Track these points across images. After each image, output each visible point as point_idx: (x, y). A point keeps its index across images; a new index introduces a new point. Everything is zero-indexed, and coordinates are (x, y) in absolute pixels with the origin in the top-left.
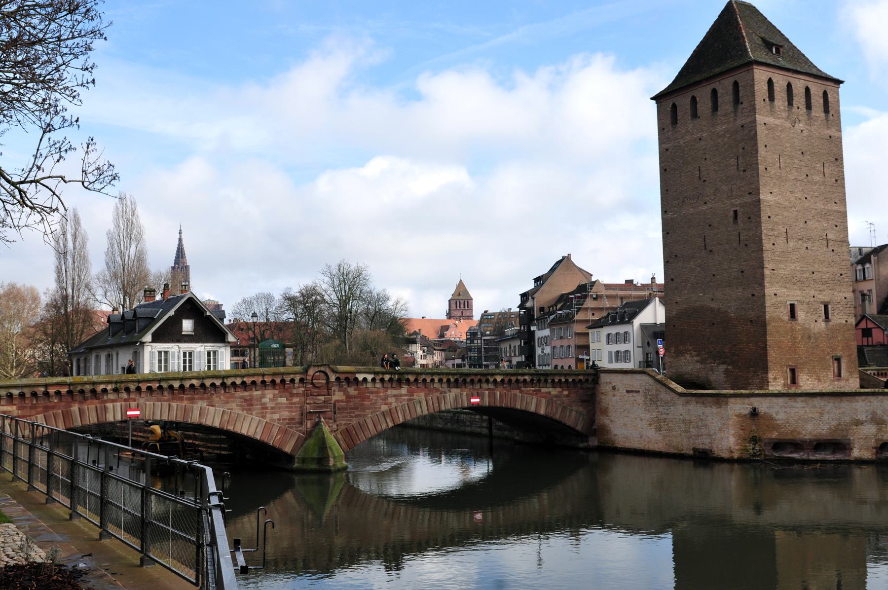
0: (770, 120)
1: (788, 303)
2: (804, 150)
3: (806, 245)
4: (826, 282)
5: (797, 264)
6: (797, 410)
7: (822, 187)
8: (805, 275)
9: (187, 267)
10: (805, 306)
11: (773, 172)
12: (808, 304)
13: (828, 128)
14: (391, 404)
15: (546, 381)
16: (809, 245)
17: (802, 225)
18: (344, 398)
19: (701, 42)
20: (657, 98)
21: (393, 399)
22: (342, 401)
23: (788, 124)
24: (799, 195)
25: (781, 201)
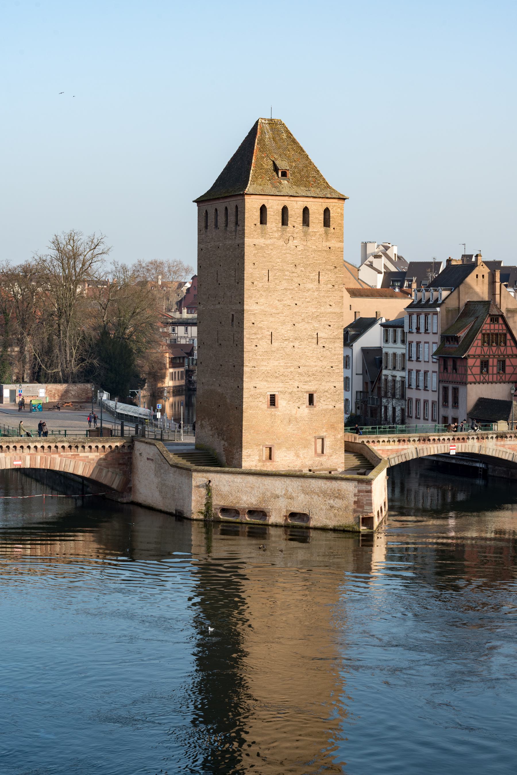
0: (261, 241)
2: (297, 262)
3: (292, 344)
4: (313, 374)
5: (281, 361)
6: (237, 485)
7: (316, 293)
11: (261, 285)
12: (290, 393)
13: (327, 240)
15: (83, 447)
16: (296, 344)
17: (289, 326)
19: (235, 155)
20: (198, 201)
23: (281, 242)
24: (288, 302)
25: (267, 309)
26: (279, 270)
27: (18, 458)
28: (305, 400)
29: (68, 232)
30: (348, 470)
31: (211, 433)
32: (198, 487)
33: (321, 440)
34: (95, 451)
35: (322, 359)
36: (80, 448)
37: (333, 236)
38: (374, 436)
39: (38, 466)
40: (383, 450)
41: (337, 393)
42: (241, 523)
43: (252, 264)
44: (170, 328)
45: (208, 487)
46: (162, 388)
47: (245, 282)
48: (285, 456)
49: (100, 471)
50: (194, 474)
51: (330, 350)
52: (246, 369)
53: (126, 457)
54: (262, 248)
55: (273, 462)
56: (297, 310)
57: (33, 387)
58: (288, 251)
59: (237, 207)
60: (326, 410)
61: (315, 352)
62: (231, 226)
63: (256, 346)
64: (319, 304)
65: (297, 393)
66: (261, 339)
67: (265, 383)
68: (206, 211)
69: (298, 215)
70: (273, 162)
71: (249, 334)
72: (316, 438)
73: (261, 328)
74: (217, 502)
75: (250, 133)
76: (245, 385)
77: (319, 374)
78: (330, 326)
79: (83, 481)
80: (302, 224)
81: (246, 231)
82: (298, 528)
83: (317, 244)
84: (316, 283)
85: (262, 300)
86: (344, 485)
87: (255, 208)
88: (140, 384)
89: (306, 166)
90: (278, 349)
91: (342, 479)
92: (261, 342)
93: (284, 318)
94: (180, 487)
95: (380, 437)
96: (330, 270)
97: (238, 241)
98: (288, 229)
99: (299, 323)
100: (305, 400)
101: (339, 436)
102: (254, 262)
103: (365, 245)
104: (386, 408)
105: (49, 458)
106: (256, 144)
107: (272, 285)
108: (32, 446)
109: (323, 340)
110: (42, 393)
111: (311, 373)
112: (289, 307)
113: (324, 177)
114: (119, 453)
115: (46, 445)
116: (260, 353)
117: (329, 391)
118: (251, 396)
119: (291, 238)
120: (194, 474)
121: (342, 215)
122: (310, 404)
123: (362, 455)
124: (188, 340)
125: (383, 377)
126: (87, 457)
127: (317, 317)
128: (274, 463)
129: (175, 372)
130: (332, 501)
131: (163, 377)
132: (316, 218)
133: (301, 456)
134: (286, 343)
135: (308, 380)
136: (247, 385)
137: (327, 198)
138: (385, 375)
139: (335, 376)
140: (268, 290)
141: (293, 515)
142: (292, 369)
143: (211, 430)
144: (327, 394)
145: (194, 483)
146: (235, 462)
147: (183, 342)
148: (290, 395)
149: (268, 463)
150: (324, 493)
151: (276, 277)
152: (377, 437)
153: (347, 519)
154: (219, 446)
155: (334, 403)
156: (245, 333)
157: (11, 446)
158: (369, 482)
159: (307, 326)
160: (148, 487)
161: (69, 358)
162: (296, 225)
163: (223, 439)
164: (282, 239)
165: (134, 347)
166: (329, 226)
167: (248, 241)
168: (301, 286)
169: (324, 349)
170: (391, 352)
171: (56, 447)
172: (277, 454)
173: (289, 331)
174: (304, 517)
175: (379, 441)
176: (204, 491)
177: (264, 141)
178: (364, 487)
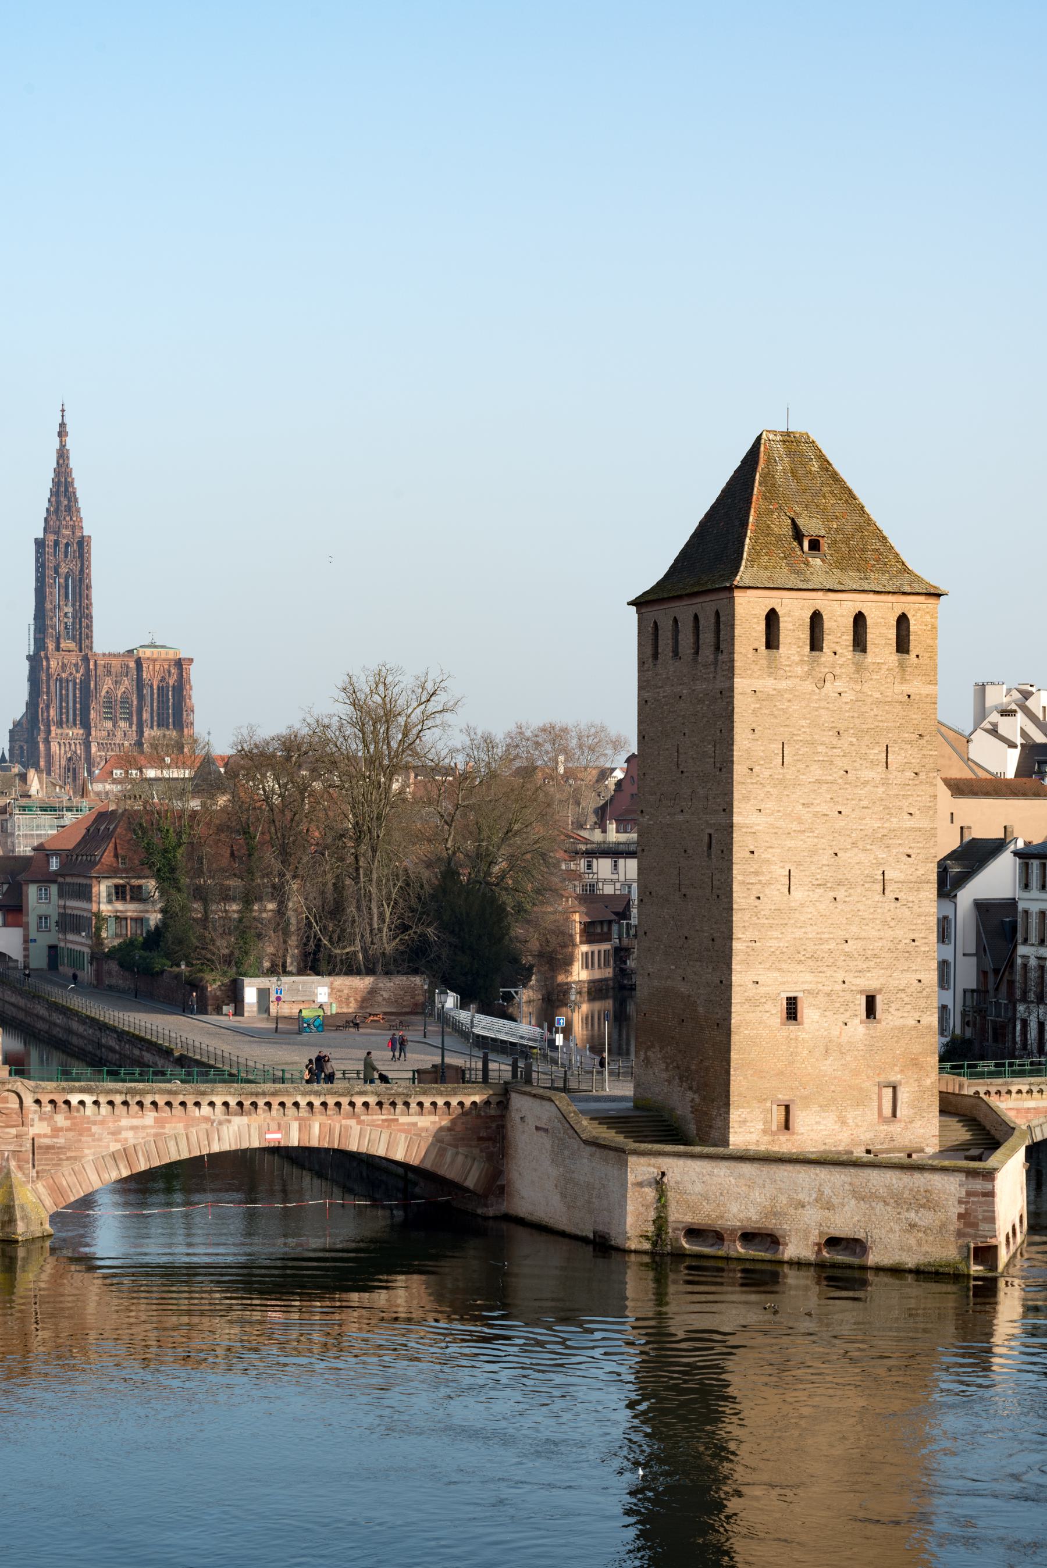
0: (767, 684)
1: (784, 995)
2: (841, 726)
3: (832, 894)
4: (875, 956)
5: (809, 929)
6: (720, 1180)
7: (881, 790)
8: (826, 947)
9: (83, 544)
10: (822, 999)
11: (767, 773)
12: (828, 995)
13: (904, 680)
14: (126, 1140)
15: (407, 1104)
16: (841, 894)
17: (826, 858)
18: (48, 1131)
19: (713, 507)
20: (639, 603)
21: (129, 1135)
22: (45, 1136)
23: (809, 686)
24: (824, 808)
26: (806, 742)
27: (274, 1126)
28: (858, 1008)
29: (374, 667)
30: (946, 1151)
31: (665, 1075)
32: (640, 1184)
33: (890, 1090)
34: (430, 1113)
35: (892, 924)
36: (400, 1107)
37: (917, 672)
38: (1000, 1081)
39: (315, 1143)
40: (1018, 1110)
41: (925, 993)
42: (727, 1259)
43: (749, 732)
44: (583, 863)
45: (659, 1184)
46: (567, 984)
47: (735, 767)
48: (818, 1123)
49: (442, 1152)
50: (632, 1160)
51: (910, 905)
52: (736, 945)
53: (494, 1125)
54: (769, 697)
55: (793, 1134)
56: (843, 824)
57: (304, 983)
58: (823, 704)
59: (717, 614)
60: (901, 1028)
61: (879, 910)
62: (707, 653)
63: (759, 898)
64: (887, 811)
65: (841, 994)
66: (769, 883)
67: (777, 974)
68: (655, 623)
69: (844, 630)
70: (793, 520)
71: (744, 873)
72: (881, 1086)
73: (767, 861)
74: (678, 1215)
75: (744, 462)
76: (736, 978)
77: (888, 955)
78: (909, 856)
79: (406, 1172)
80: (851, 648)
81: (736, 664)
82: (843, 1267)
83: (882, 689)
84: (882, 768)
85: (769, 805)
86: (937, 1180)
87: (755, 616)
88: (522, 977)
89: (860, 529)
90: (802, 905)
91: (934, 1169)
92: (767, 891)
93: (816, 840)
94: (604, 1186)
95: (1011, 1084)
96: (910, 742)
97: (720, 685)
98: (823, 659)
99: (846, 850)
100: (858, 1008)
101: (928, 1082)
102: (754, 726)
103: (981, 690)
104: (1025, 1023)
105: (338, 1126)
106: (757, 484)
107: (790, 773)
108: (303, 1103)
109: (896, 885)
110: (323, 993)
111: (869, 952)
112: (825, 818)
113: (897, 549)
114: (479, 1116)
115: (331, 1101)
116: (767, 912)
117: (908, 990)
118: (748, 1000)
119: (829, 677)
120: (632, 1160)
121: (934, 627)
122: (868, 1017)
123: (975, 1120)
124: (618, 886)
125: (1019, 961)
126: (415, 1124)
127: (882, 839)
128: (795, 1137)
129: (593, 953)
130: (912, 1215)
131: (569, 962)
132: (881, 635)
133: (850, 1121)
134: (820, 891)
135: (865, 966)
136: (741, 977)
137: (904, 593)
138: (1023, 956)
139: (919, 960)
140: (781, 782)
141: (833, 1242)
142: (832, 945)
143: (667, 1069)
144: (903, 995)
145: (631, 1178)
146: (715, 1134)
147: (608, 890)
148: (827, 999)
149: (783, 1137)
150: (898, 1200)
151: (799, 757)
152: (1006, 1084)
153: (945, 1251)
154: (681, 1103)
155: (917, 1014)
156: (734, 872)
157: (261, 1102)
158: (989, 1175)
159: (862, 856)
160: (537, 1186)
161: (376, 925)
162: (839, 651)
163: (690, 1088)
164: (810, 680)
165: (508, 901)
166: (907, 652)
167: (741, 684)
168: (849, 775)
169: (898, 904)
170: (1034, 908)
171: (352, 1104)
172: (801, 1119)
173: (825, 868)
174: (855, 1245)
175: (1009, 1092)
176: (650, 1193)
177: (773, 477)
178: (978, 1185)
